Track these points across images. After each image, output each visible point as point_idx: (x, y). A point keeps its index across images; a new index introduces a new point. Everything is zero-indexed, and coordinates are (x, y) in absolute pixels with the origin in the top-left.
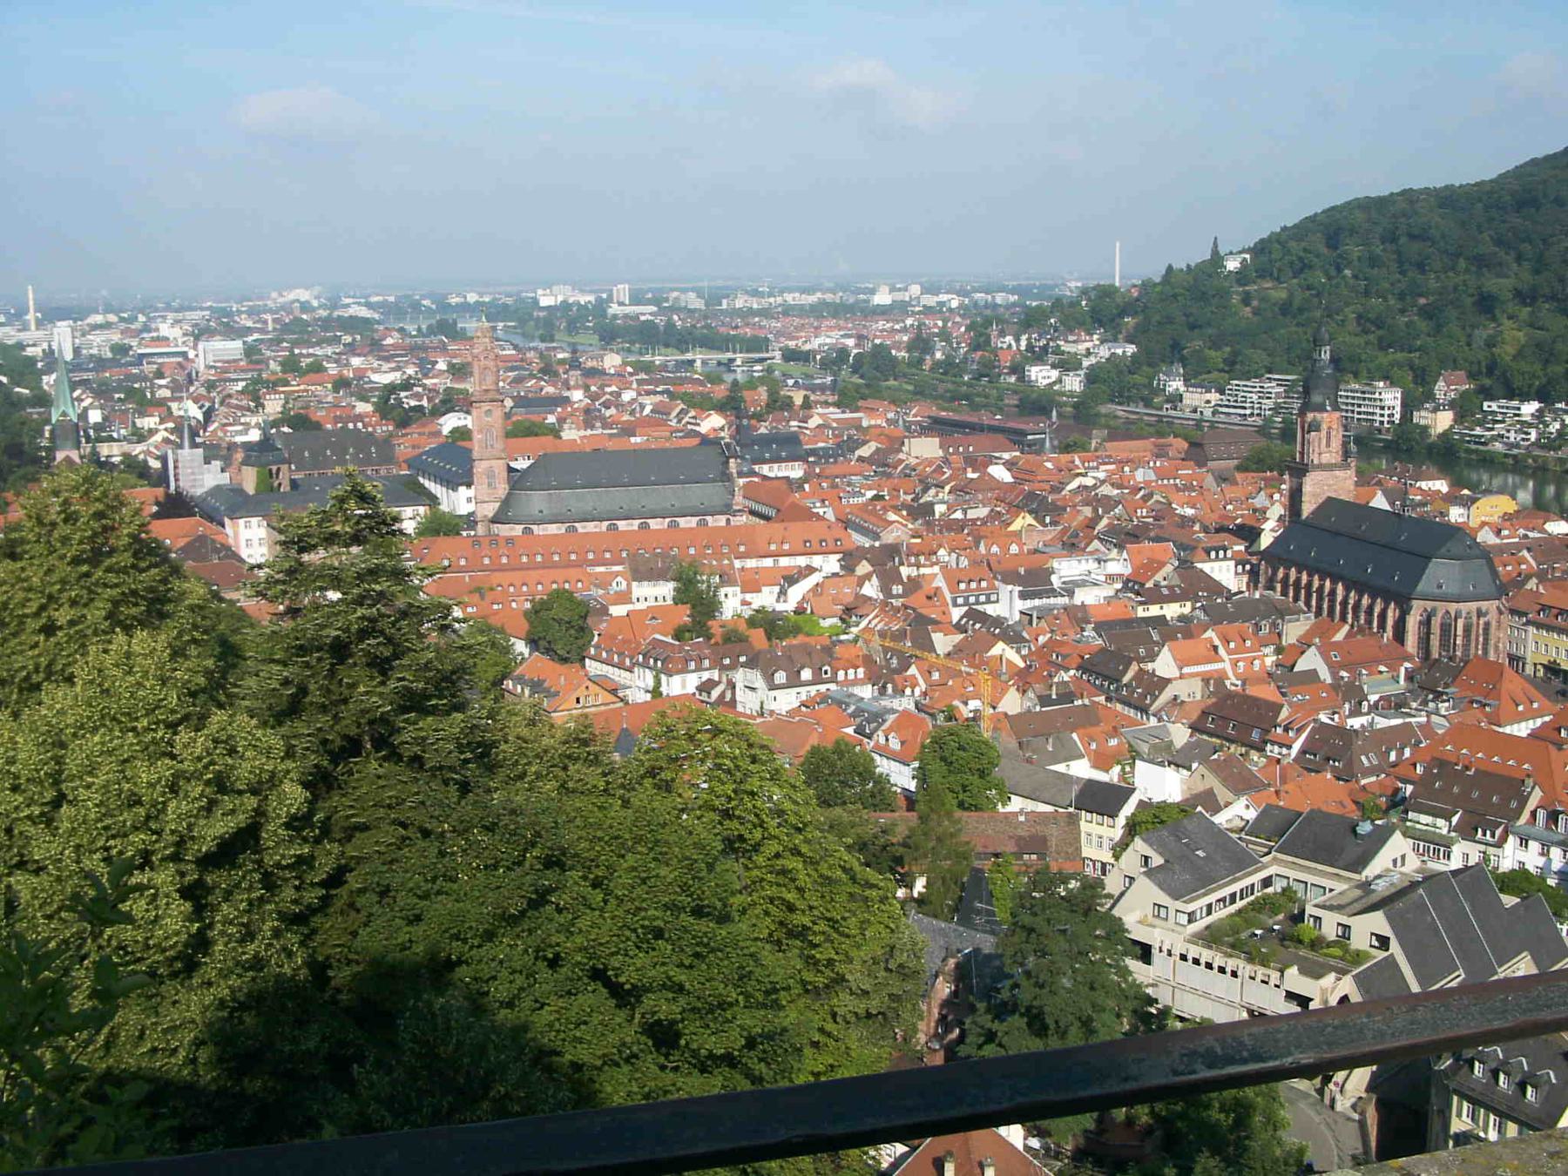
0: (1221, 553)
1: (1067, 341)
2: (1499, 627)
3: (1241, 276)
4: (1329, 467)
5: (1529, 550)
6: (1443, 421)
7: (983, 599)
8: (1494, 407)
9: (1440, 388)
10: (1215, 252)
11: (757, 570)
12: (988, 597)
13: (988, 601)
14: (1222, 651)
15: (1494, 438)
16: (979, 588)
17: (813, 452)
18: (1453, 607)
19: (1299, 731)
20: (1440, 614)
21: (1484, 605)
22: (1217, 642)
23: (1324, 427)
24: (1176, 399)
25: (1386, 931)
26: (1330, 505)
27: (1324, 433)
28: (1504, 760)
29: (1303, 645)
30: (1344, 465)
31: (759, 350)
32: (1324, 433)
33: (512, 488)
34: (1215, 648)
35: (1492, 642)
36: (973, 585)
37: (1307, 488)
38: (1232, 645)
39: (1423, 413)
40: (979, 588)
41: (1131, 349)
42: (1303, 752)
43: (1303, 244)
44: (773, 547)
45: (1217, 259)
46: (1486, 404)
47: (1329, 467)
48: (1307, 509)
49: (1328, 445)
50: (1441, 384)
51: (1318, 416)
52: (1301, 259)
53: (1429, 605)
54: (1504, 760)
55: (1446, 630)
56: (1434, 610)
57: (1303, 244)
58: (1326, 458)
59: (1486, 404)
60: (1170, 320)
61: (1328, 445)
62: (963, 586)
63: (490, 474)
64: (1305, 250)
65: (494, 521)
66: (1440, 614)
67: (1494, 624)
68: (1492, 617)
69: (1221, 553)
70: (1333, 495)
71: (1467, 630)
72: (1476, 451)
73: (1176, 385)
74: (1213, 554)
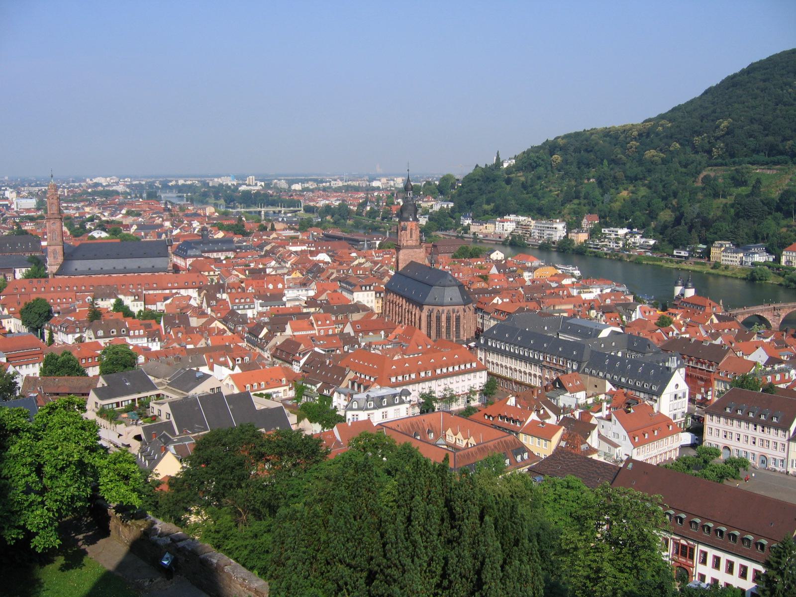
0: (368, 288)
1: (423, 201)
2: (464, 318)
3: (509, 170)
4: (411, 247)
5: (522, 288)
6: (582, 237)
7: (247, 307)
8: (607, 232)
9: (584, 222)
10: (498, 159)
11: (155, 295)
12: (249, 306)
13: (250, 308)
14: (315, 325)
15: (603, 246)
16: (245, 302)
17: (240, 248)
18: (440, 308)
19: (304, 355)
20: (445, 312)
21: (456, 308)
22: (313, 321)
23: (409, 228)
24: (466, 229)
25: (170, 412)
26: (412, 265)
27: (408, 231)
28: (369, 364)
29: (486, 342)
30: (420, 246)
31: (294, 207)
32: (408, 231)
33: (64, 260)
34: (312, 324)
35: (462, 325)
36: (243, 301)
37: (401, 257)
38: (320, 323)
39: (573, 234)
40: (245, 302)
41: (451, 205)
42: (305, 364)
43: (537, 154)
44: (170, 285)
45: (499, 163)
46: (603, 230)
47: (411, 247)
48: (400, 269)
49: (411, 236)
50: (585, 220)
51: (406, 223)
52: (535, 162)
53: (431, 307)
54: (369, 364)
55: (438, 319)
56: (433, 309)
57: (537, 154)
58: (410, 243)
59: (603, 230)
60: (471, 191)
61: (411, 236)
62: (237, 301)
63: (55, 252)
64: (537, 157)
65: (56, 274)
66: (445, 312)
67: (462, 317)
68: (461, 313)
69: (368, 288)
70: (414, 260)
71: (448, 319)
72: (595, 252)
73: (467, 222)
74: (364, 288)
